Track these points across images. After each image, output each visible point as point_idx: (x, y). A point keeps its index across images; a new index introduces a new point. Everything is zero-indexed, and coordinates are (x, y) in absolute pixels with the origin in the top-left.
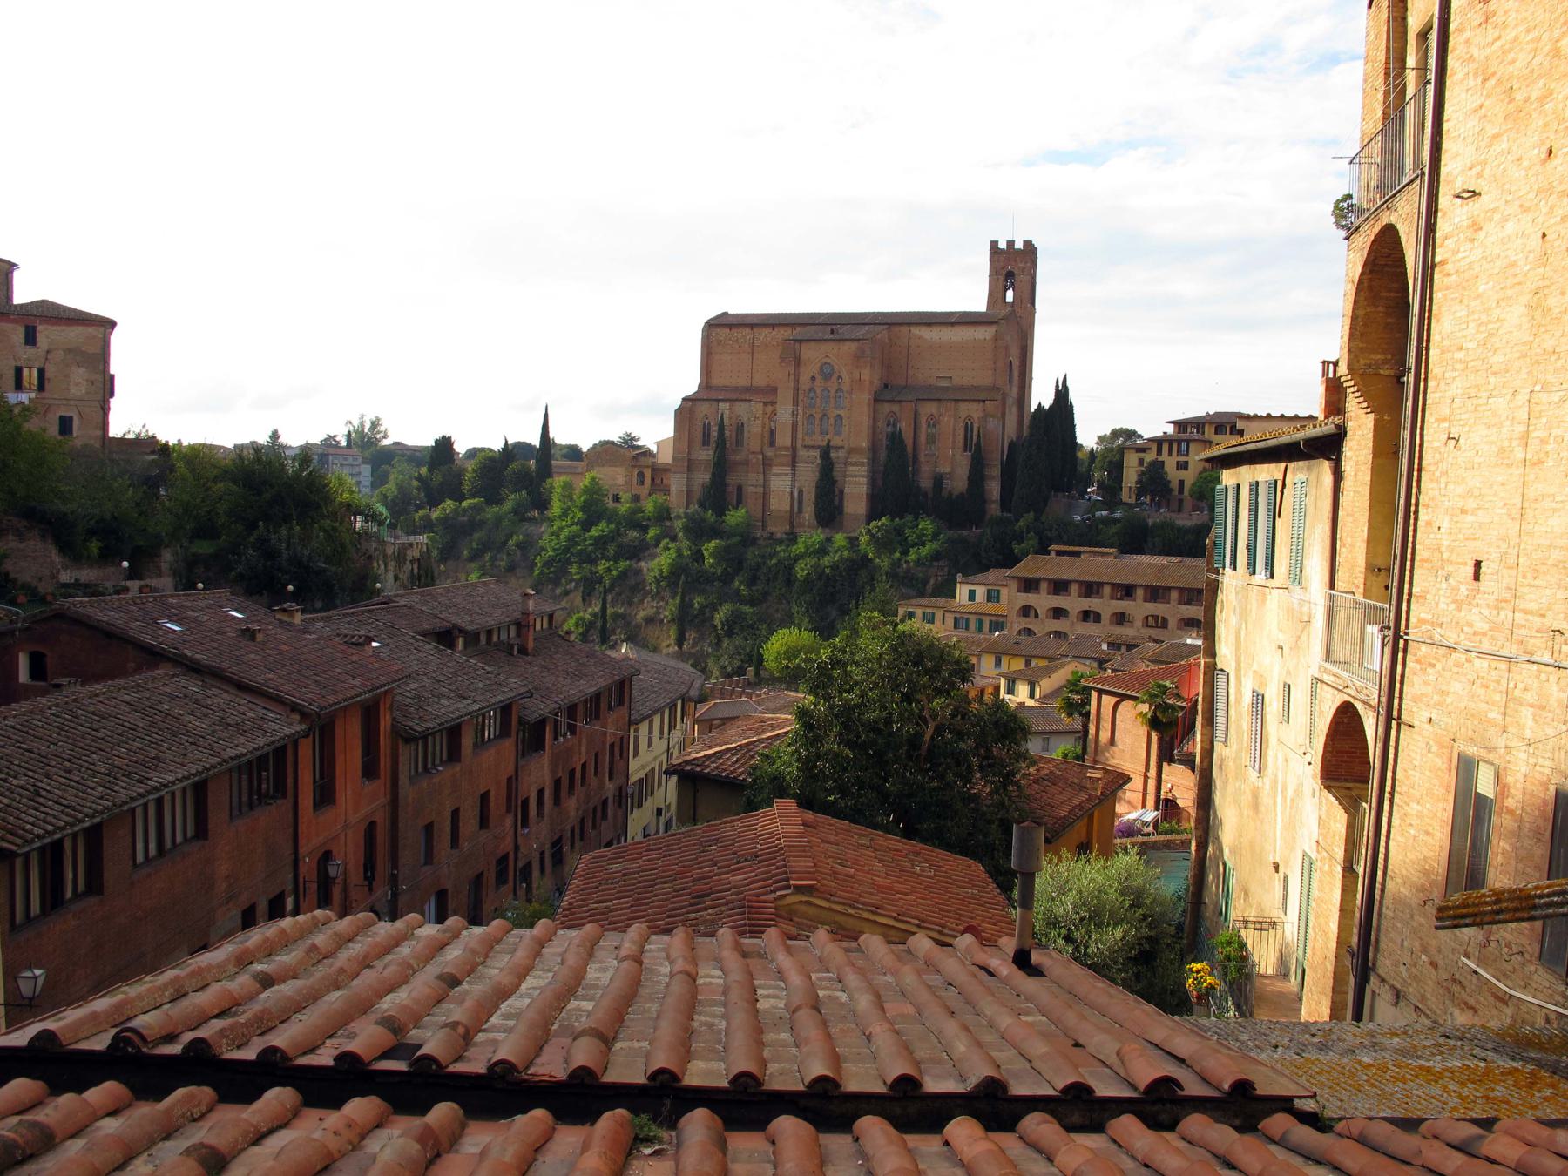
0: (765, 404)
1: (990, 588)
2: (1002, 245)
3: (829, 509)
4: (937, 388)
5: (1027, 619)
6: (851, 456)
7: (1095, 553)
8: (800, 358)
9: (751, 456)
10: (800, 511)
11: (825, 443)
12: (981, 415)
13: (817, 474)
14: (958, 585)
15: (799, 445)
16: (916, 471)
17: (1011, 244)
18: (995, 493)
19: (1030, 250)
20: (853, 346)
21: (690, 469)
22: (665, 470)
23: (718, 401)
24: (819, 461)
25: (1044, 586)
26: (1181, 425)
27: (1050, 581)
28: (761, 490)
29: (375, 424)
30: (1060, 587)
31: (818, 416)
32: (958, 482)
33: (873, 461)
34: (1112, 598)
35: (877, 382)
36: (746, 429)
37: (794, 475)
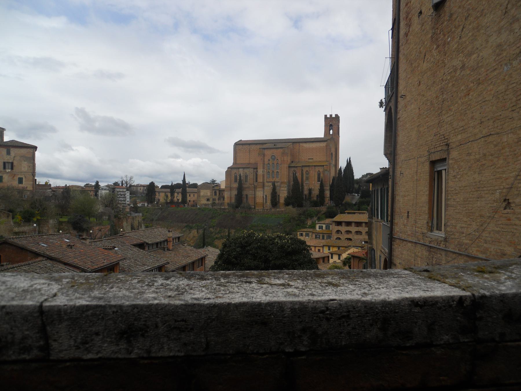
0: (254, 169)
2: (328, 116)
3: (275, 202)
5: (339, 235)
7: (360, 213)
10: (266, 202)
13: (271, 190)
15: (265, 181)
16: (303, 188)
17: (331, 115)
19: (337, 117)
20: (281, 150)
21: (231, 190)
22: (223, 190)
23: (239, 168)
25: (343, 224)
27: (345, 222)
28: (253, 196)
29: (131, 178)
30: (348, 224)
31: (271, 172)
32: (316, 192)
33: (289, 186)
34: (365, 227)
35: (289, 161)
36: (248, 177)
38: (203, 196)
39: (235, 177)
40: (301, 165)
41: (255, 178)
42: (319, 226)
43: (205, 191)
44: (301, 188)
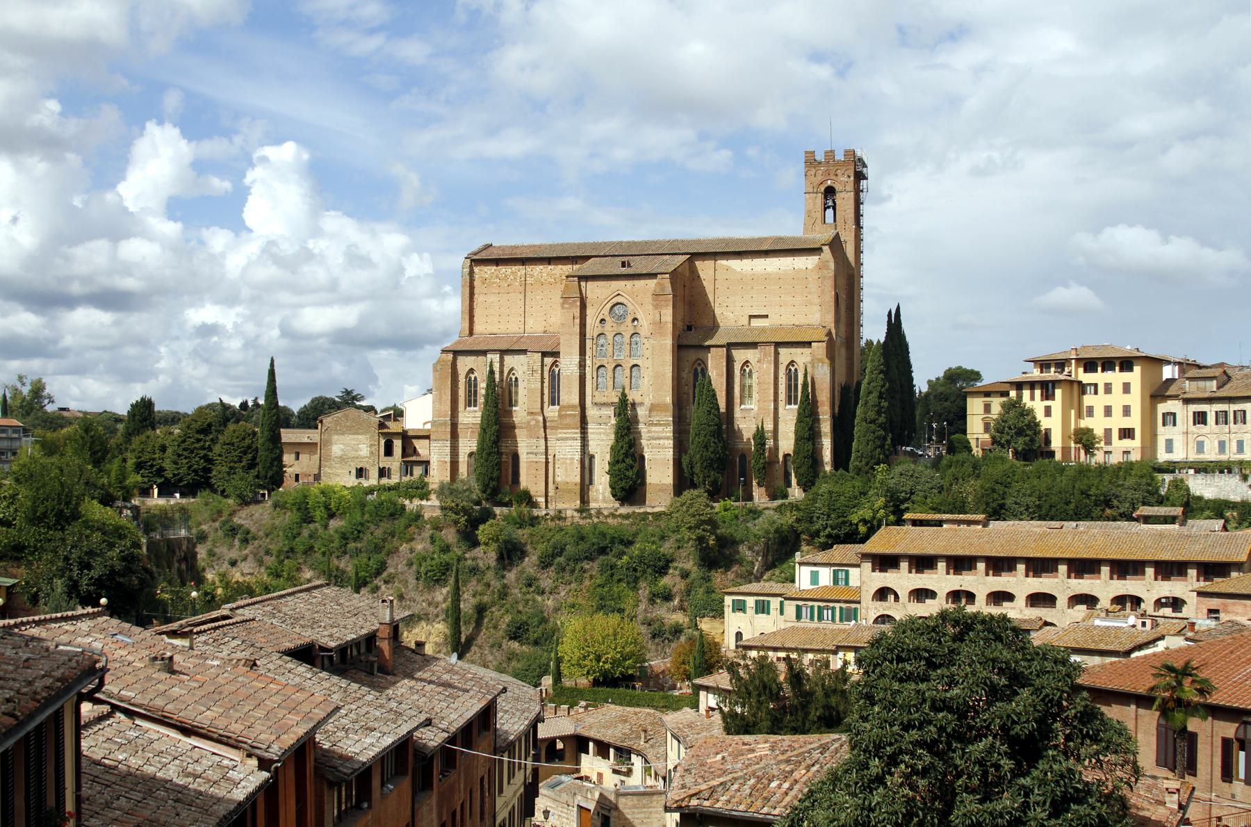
0: (544, 354)
4: (752, 330)
6: (654, 413)
7: (959, 522)
8: (586, 298)
12: (809, 359)
13: (613, 436)
14: (797, 566)
17: (830, 154)
20: (652, 283)
23: (484, 353)
24: (613, 421)
26: (1044, 365)
31: (610, 367)
35: (680, 324)
38: (341, 457)
40: (723, 341)
41: (546, 391)
43: (349, 439)
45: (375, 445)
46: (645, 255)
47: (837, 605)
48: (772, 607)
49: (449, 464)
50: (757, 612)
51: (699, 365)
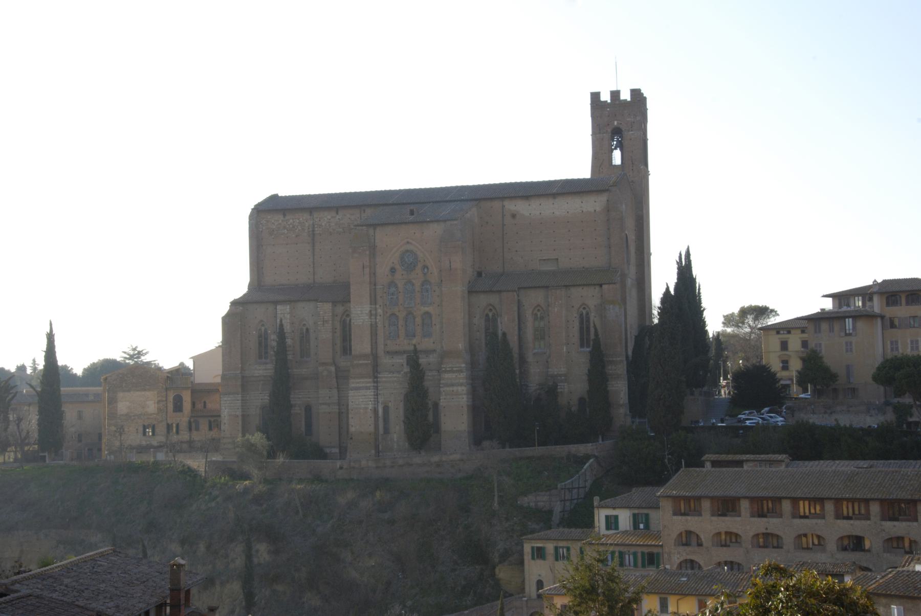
1: (636, 511)
2: (606, 97)
5: (688, 549)
9: (320, 369)
10: (387, 431)
11: (412, 348)
14: (596, 511)
17: (615, 94)
18: (622, 395)
24: (406, 369)
33: (473, 365)
37: (376, 388)
39: (260, 336)
42: (607, 517)
44: (517, 371)
45: (163, 401)
46: (433, 202)
47: (639, 550)
48: (572, 552)
49: (240, 418)
50: (557, 559)
51: (491, 310)
